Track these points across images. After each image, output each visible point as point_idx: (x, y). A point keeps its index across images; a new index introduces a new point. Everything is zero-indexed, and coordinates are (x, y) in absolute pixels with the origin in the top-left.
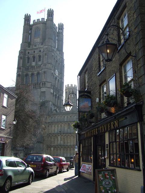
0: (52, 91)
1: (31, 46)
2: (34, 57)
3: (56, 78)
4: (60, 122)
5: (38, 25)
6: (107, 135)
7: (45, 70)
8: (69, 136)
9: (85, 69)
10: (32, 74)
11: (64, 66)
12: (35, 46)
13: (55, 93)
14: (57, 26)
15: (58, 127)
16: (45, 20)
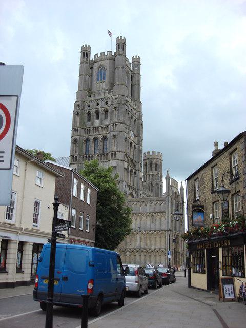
0: (126, 165)
1: (92, 95)
2: (97, 113)
3: (131, 144)
4: (140, 213)
5: (103, 63)
6: (220, 250)
7: (116, 133)
8: (153, 235)
9: (196, 177)
10: (96, 139)
11: (142, 124)
12: (99, 95)
13: (130, 168)
14: (131, 61)
15: (136, 220)
16: (113, 54)
